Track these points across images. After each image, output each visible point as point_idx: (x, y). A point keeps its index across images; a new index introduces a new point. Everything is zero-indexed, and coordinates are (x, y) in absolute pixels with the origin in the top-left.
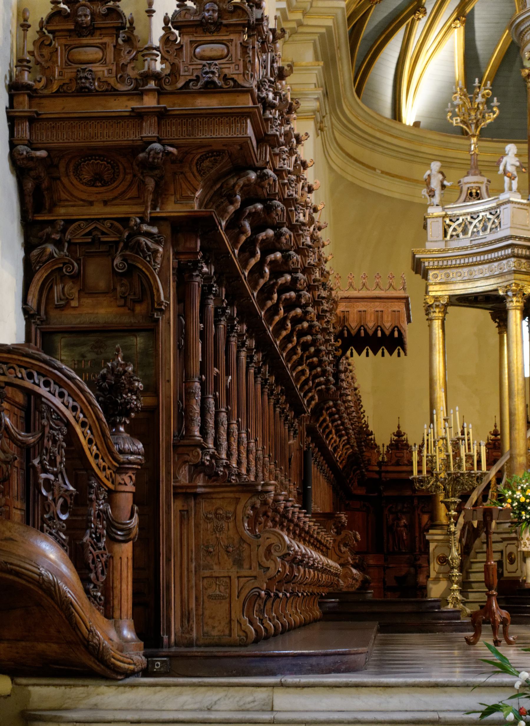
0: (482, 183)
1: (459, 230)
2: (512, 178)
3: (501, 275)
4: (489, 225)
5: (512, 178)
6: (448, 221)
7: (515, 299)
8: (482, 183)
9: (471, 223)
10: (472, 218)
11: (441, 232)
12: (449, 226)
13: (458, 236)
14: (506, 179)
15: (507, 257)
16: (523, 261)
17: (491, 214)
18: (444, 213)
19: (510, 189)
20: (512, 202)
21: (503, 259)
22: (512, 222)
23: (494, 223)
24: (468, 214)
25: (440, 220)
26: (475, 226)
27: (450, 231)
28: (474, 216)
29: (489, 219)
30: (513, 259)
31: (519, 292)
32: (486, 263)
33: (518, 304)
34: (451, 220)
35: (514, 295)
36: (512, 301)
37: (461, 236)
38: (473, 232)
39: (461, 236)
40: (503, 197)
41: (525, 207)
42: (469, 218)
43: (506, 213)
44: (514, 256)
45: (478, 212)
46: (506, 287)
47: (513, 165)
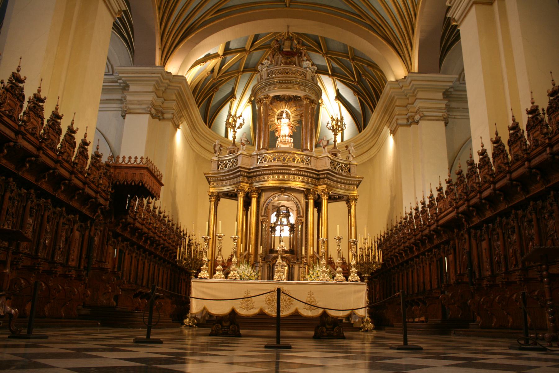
0: (236, 149)
1: (224, 166)
2: (244, 145)
3: (237, 183)
4: (234, 164)
5: (244, 145)
6: (220, 163)
7: (240, 193)
8: (236, 149)
9: (228, 163)
10: (229, 161)
11: (217, 167)
12: (220, 165)
13: (223, 168)
14: (241, 145)
15: (239, 176)
16: (246, 178)
17: (235, 159)
18: (218, 159)
19: (243, 149)
20: (242, 154)
21: (238, 177)
22: (242, 162)
23: (236, 163)
24: (227, 160)
25: (217, 162)
26: (230, 165)
27: (220, 167)
28: (229, 160)
29: (235, 162)
30: (241, 177)
31: (242, 190)
32: (232, 179)
33: (242, 195)
34: (221, 162)
35: (240, 191)
36: (239, 194)
37: (224, 168)
38: (228, 167)
39: (224, 168)
40: (239, 153)
41: (248, 157)
42: (227, 161)
43: (240, 159)
44: (241, 176)
45: (230, 159)
46: (237, 188)
47: (244, 140)
